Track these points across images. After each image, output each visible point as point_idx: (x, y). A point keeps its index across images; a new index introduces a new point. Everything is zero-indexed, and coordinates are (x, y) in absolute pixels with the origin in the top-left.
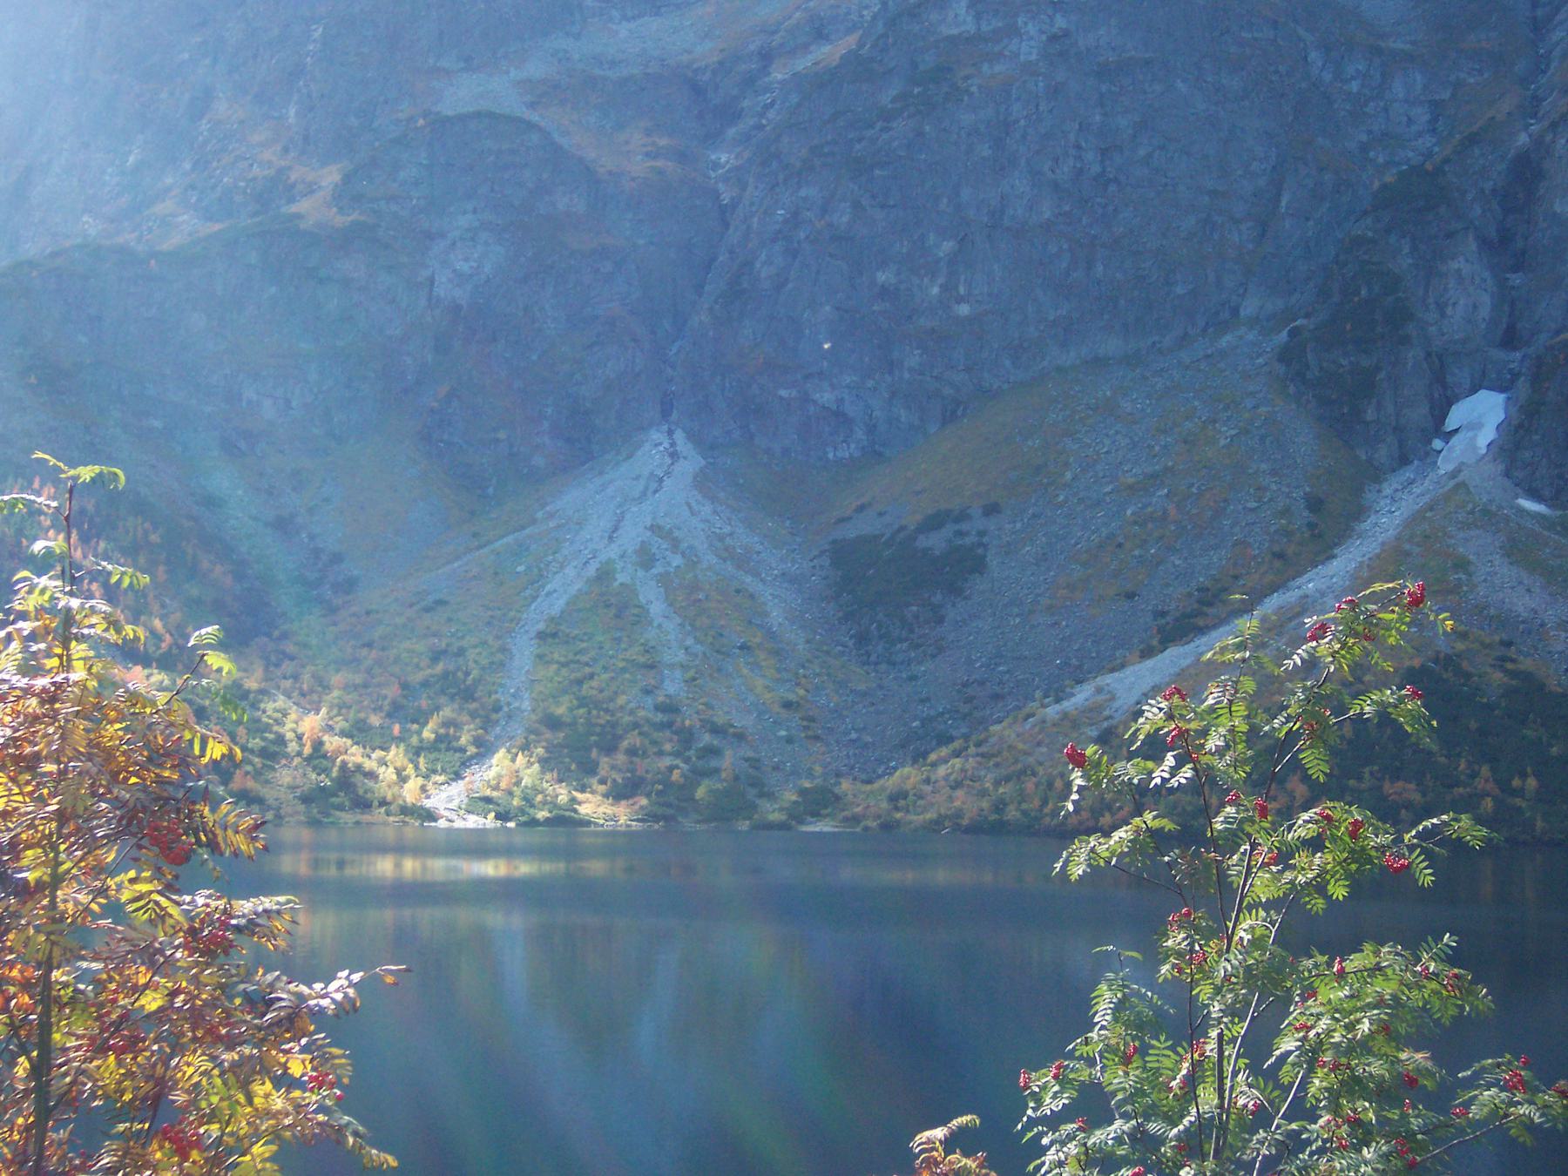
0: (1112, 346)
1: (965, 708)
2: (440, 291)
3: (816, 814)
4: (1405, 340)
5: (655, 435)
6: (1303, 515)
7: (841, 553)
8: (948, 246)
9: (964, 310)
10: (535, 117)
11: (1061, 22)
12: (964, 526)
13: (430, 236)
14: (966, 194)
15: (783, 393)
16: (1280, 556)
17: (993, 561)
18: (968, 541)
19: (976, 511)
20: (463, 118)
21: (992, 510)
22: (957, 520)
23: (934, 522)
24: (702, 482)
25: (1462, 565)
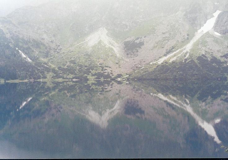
1: (140, 63)
3: (119, 77)
5: (101, 28)
12: (141, 39)
15: (118, 22)
18: (142, 41)
19: (143, 37)
21: (145, 37)
22: (140, 38)
25: (207, 42)
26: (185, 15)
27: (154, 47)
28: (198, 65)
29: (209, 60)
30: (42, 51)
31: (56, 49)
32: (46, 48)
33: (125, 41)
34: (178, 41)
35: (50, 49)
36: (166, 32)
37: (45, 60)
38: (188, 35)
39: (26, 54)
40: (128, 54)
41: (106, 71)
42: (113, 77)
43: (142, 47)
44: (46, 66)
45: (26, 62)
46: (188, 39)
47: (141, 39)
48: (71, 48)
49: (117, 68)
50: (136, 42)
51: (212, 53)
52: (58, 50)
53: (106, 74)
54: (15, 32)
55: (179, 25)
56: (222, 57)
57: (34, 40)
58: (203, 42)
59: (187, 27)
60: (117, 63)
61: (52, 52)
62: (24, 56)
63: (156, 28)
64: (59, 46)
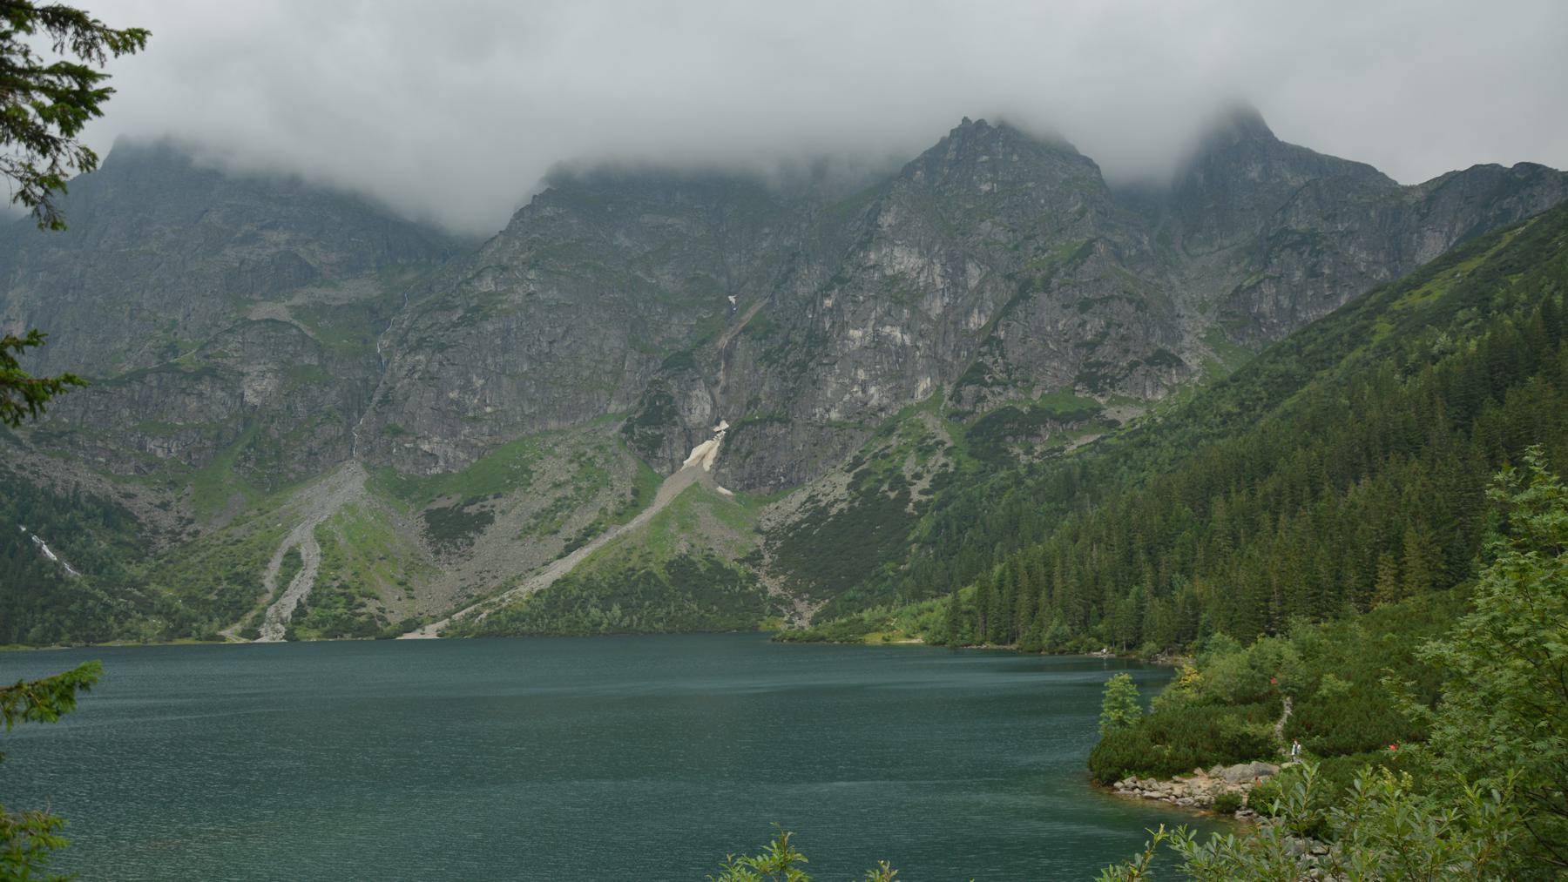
0: (553, 425)
2: (246, 399)
4: (675, 424)
6: (629, 497)
7: (430, 516)
8: (481, 382)
9: (489, 409)
10: (295, 322)
11: (532, 288)
13: (242, 374)
14: (489, 361)
16: (620, 515)
17: (497, 518)
20: (259, 322)
24: (369, 485)
26: (627, 430)
27: (528, 530)
29: (702, 570)
30: (126, 538)
31: (180, 533)
32: (141, 530)
33: (429, 507)
34: (603, 510)
35: (155, 532)
36: (567, 482)
37: (138, 571)
38: (635, 492)
39: (58, 548)
40: (437, 553)
41: (363, 610)
43: (489, 528)
44: (137, 593)
45: (59, 579)
46: (635, 505)
48: (233, 530)
52: (184, 537)
53: (363, 619)
54: (20, 467)
55: (607, 461)
56: (741, 561)
57: (92, 498)
58: (679, 514)
59: (632, 465)
60: (401, 584)
61: (163, 543)
62: (52, 556)
63: (532, 467)
64: (191, 521)
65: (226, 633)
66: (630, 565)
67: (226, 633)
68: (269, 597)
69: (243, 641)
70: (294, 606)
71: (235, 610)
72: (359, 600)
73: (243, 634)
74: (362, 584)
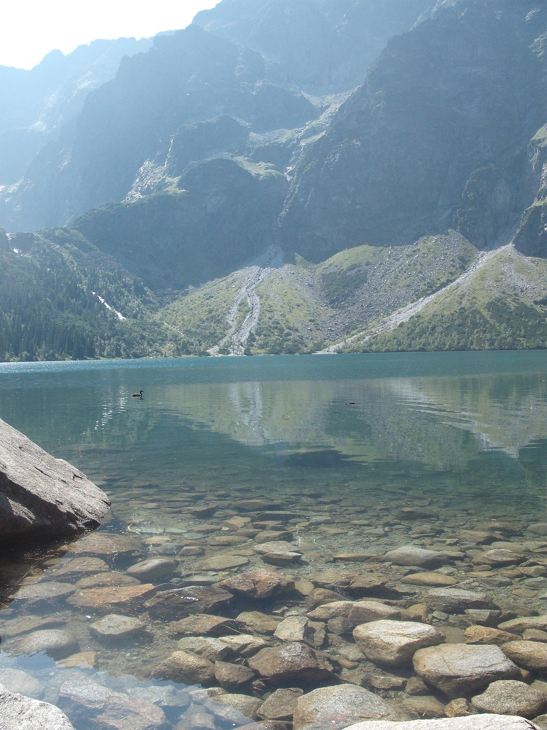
9: (358, 207)
22: (359, 267)
23: (352, 268)
28: (492, 321)
29: (513, 308)
39: (112, 304)
42: (305, 350)
47: (360, 269)
49: (311, 330)
50: (349, 276)
51: (516, 295)
53: (290, 343)
56: (536, 303)
65: (210, 351)
66: (463, 306)
67: (210, 351)
68: (233, 329)
69: (220, 355)
70: (248, 334)
71: (214, 338)
72: (287, 331)
73: (221, 351)
74: (288, 321)
